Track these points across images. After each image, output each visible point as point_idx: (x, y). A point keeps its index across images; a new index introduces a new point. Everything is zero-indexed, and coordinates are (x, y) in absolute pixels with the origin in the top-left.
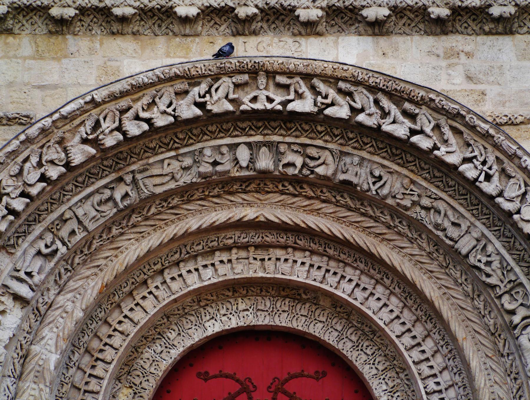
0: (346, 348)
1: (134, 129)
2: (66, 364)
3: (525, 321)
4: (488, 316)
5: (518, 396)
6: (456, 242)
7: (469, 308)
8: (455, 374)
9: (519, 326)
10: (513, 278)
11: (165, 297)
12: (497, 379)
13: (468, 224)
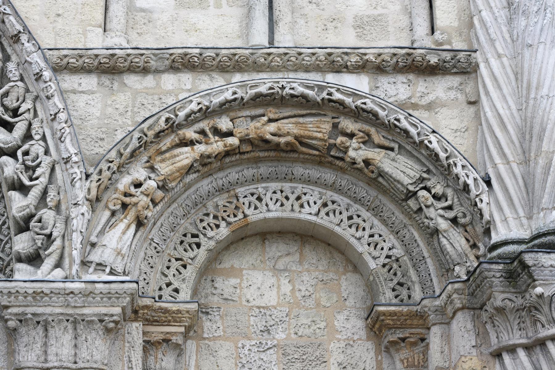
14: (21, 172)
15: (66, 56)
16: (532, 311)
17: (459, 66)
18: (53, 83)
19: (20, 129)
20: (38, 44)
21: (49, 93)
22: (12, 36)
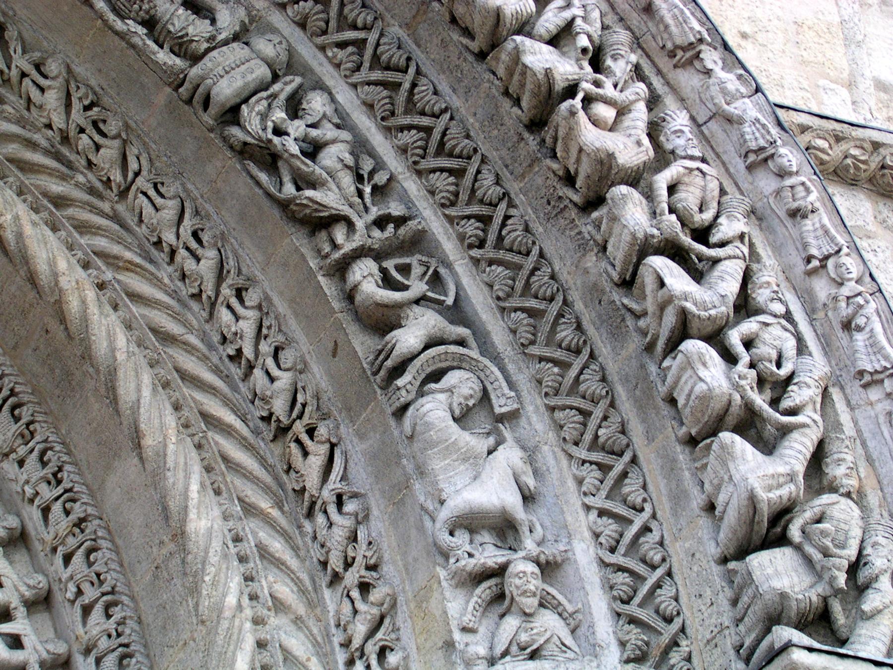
3: (441, 349)
4: (270, 363)
5: (372, 649)
6: (196, 59)
7: (193, 339)
8: (87, 610)
9: (417, 363)
10: (396, 209)
12: (286, 591)
13: (242, 13)
14: (752, 388)
15: (804, 129)
18: (810, 180)
19: (727, 282)
20: (754, 79)
21: (801, 203)
22: (677, 47)
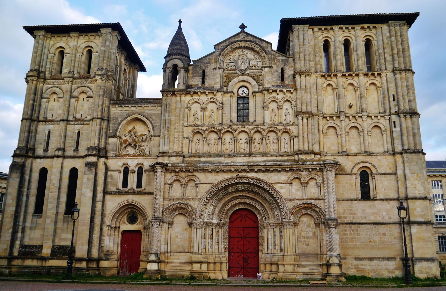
0: (254, 211)
1: (226, 185)
2: (219, 213)
11: (231, 205)
16: (329, 225)
17: (323, 199)
